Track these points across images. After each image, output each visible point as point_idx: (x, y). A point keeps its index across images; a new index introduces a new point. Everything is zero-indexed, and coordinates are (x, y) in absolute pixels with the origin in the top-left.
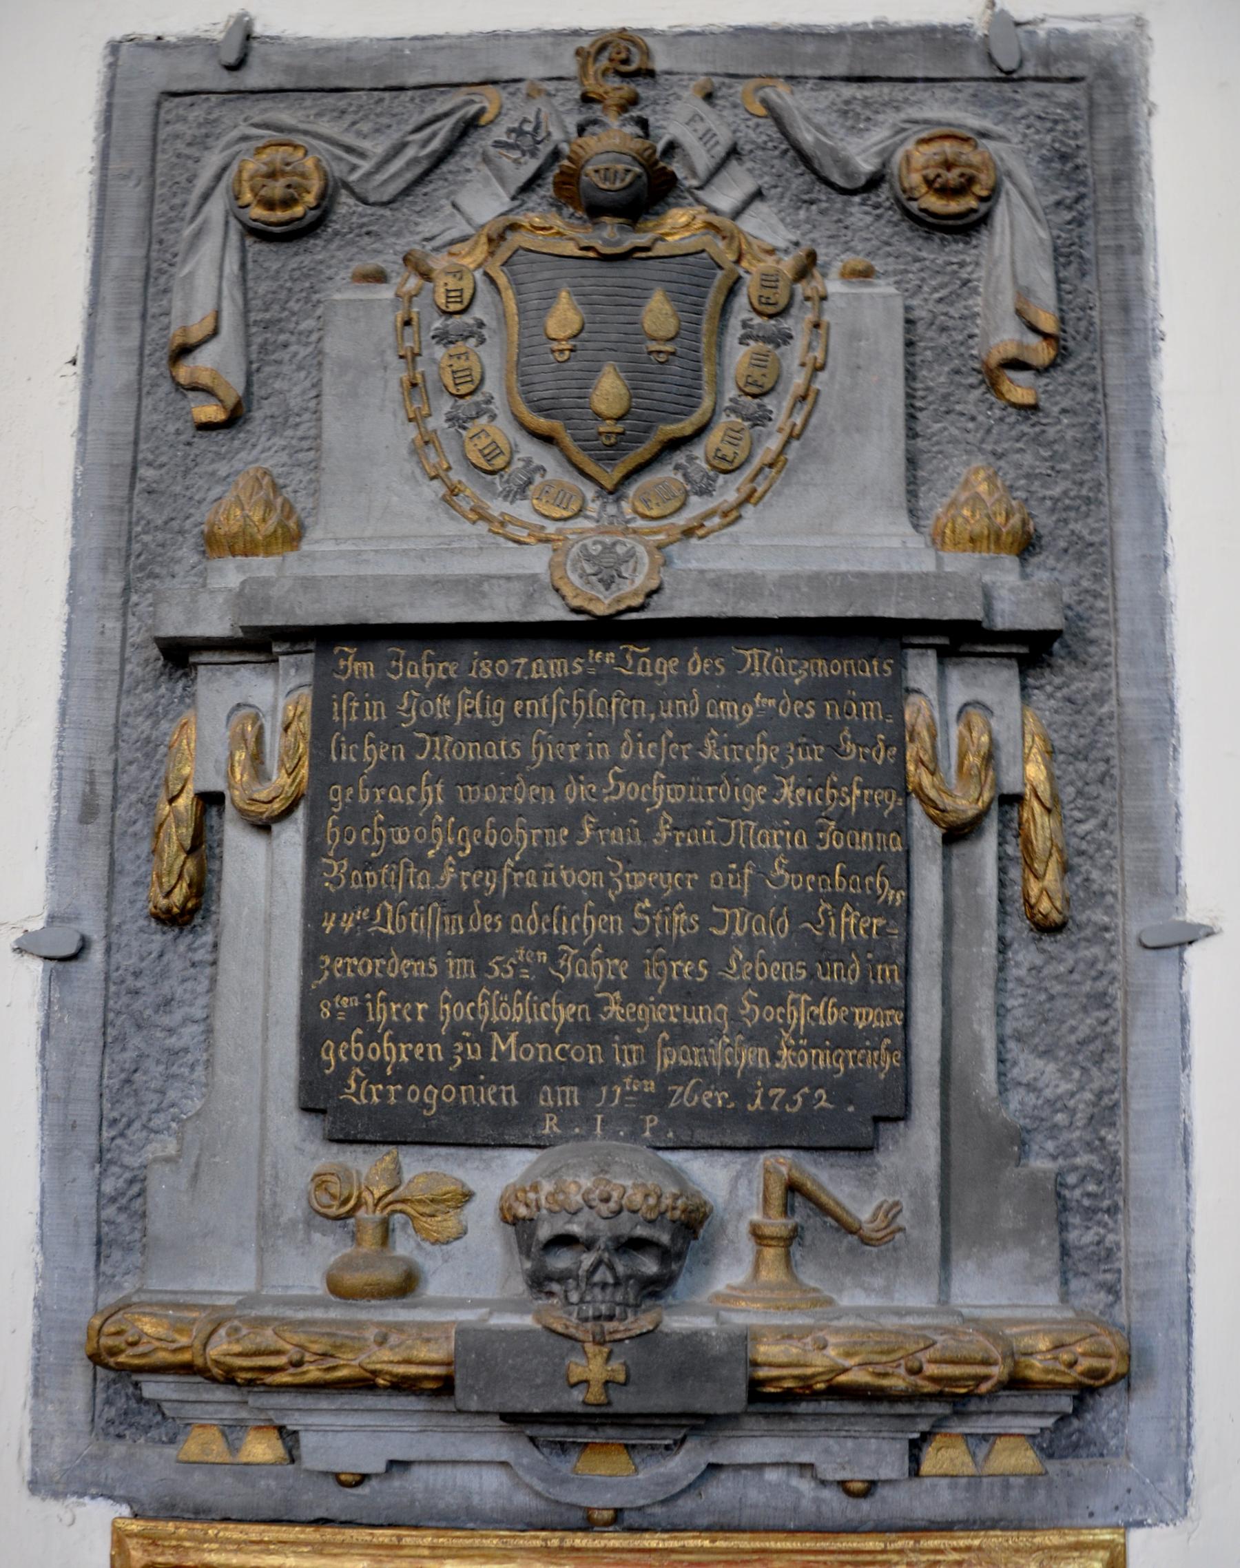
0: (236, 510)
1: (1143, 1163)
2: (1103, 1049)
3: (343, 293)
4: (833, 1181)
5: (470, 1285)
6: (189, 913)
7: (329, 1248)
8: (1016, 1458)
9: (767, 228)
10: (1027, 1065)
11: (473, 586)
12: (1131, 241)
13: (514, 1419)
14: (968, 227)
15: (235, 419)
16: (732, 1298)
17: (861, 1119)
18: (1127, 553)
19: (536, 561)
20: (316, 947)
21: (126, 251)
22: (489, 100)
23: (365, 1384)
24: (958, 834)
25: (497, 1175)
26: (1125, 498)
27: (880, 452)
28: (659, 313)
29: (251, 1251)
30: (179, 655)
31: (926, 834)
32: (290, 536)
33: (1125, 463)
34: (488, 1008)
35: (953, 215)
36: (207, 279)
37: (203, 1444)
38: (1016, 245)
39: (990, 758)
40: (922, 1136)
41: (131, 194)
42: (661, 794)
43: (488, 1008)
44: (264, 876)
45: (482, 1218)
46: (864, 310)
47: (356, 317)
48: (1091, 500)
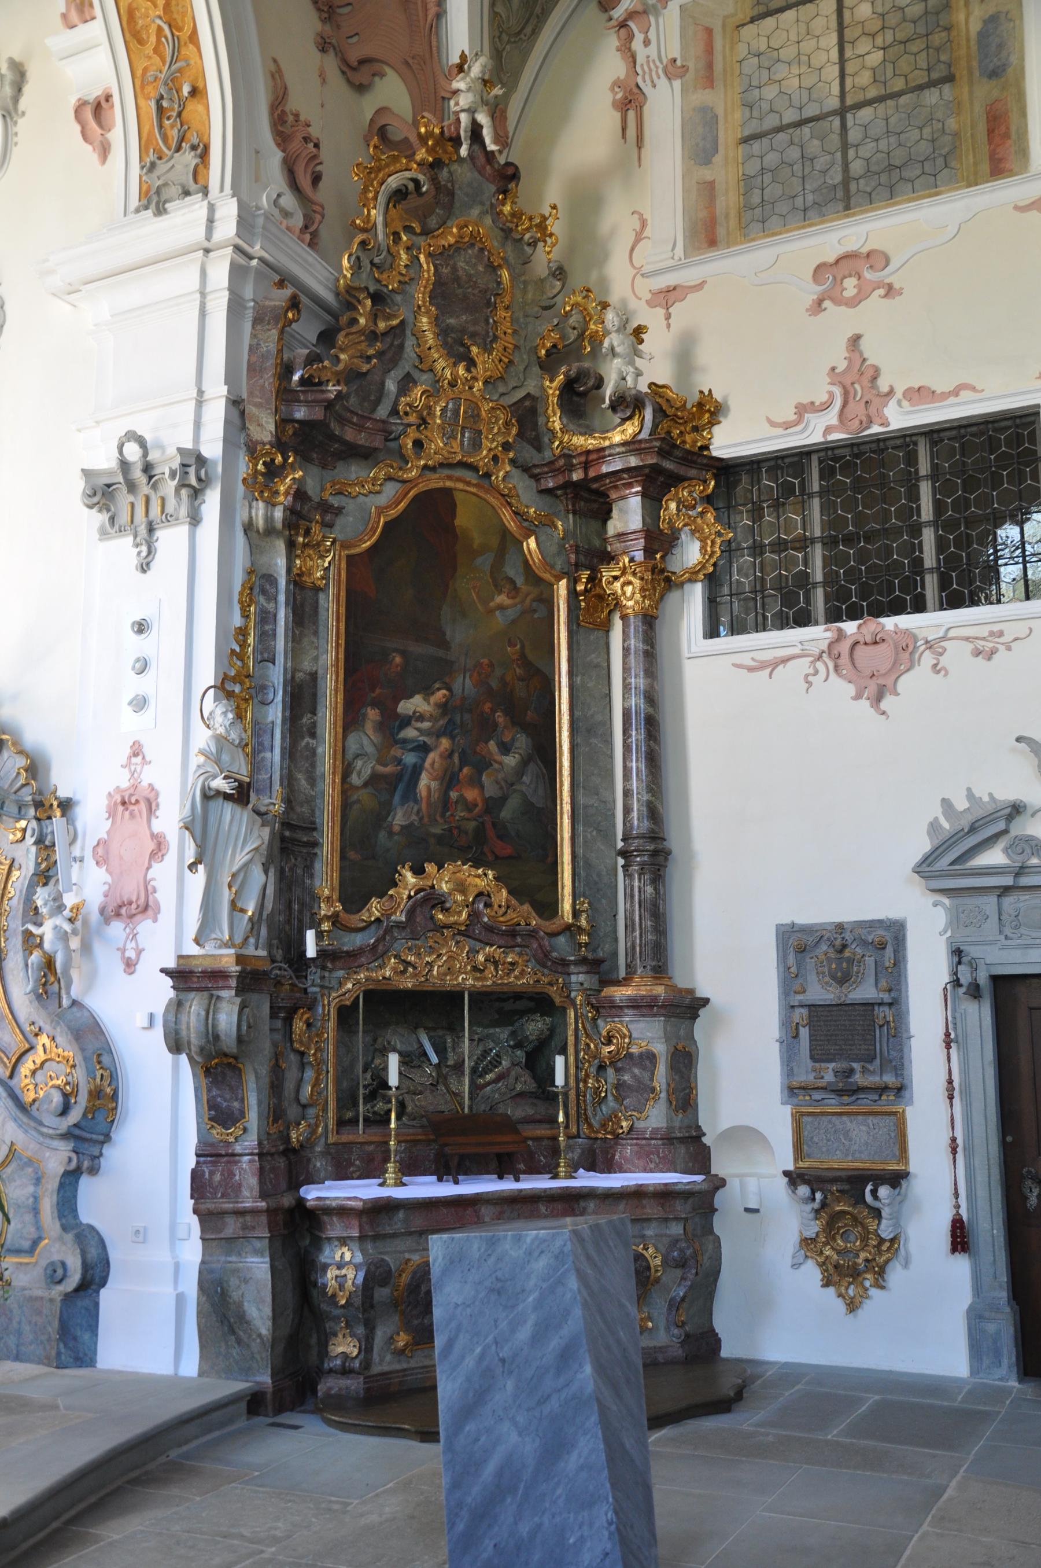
0: (797, 988)
1: (906, 1064)
2: (901, 1050)
3: (808, 960)
4: (868, 1066)
5: (829, 1077)
6: (796, 1036)
7: (814, 1074)
8: (892, 1098)
9: (858, 950)
10: (892, 1052)
11: (825, 1000)
12: (905, 949)
13: (833, 1091)
14: (884, 948)
15: (797, 976)
16: (858, 1078)
17: (871, 1059)
18: (903, 990)
19: (832, 996)
20: (811, 1041)
21: (781, 953)
22: (824, 932)
23: (818, 1088)
24: (881, 1026)
25: (832, 1065)
26: (903, 983)
27: (872, 980)
28: (845, 965)
29: (805, 1076)
30: (793, 1007)
31: (877, 1027)
32: (804, 992)
33: (903, 979)
34: (829, 1047)
35: (882, 946)
36: (791, 960)
37: (801, 1098)
38: (889, 951)
39: (885, 1017)
40: (878, 1061)
41: (781, 945)
42: (847, 1023)
43: (829, 1047)
44: (804, 1032)
45: (830, 1070)
46: (870, 961)
47: (810, 963)
48: (899, 984)
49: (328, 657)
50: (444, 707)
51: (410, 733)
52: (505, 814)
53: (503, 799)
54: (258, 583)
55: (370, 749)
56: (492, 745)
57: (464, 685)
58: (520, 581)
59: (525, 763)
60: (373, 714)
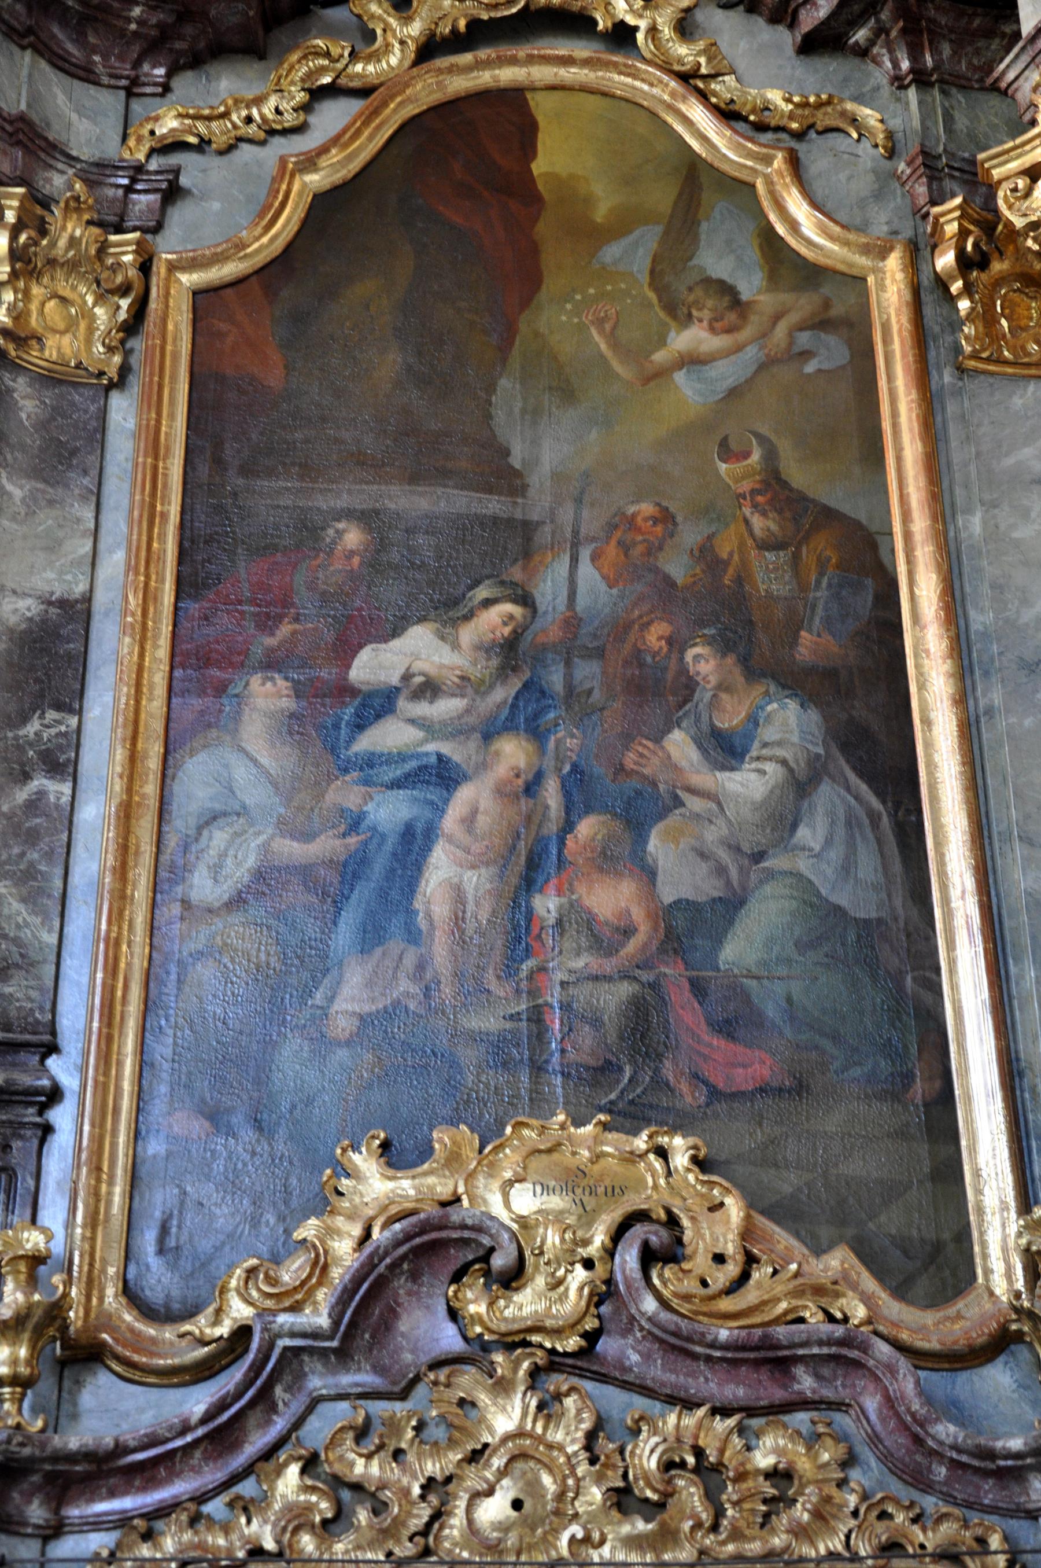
50: (510, 651)
51: (391, 735)
52: (739, 949)
53: (731, 906)
55: (252, 791)
56: (680, 745)
58: (750, 284)
59: (801, 785)
60: (267, 696)
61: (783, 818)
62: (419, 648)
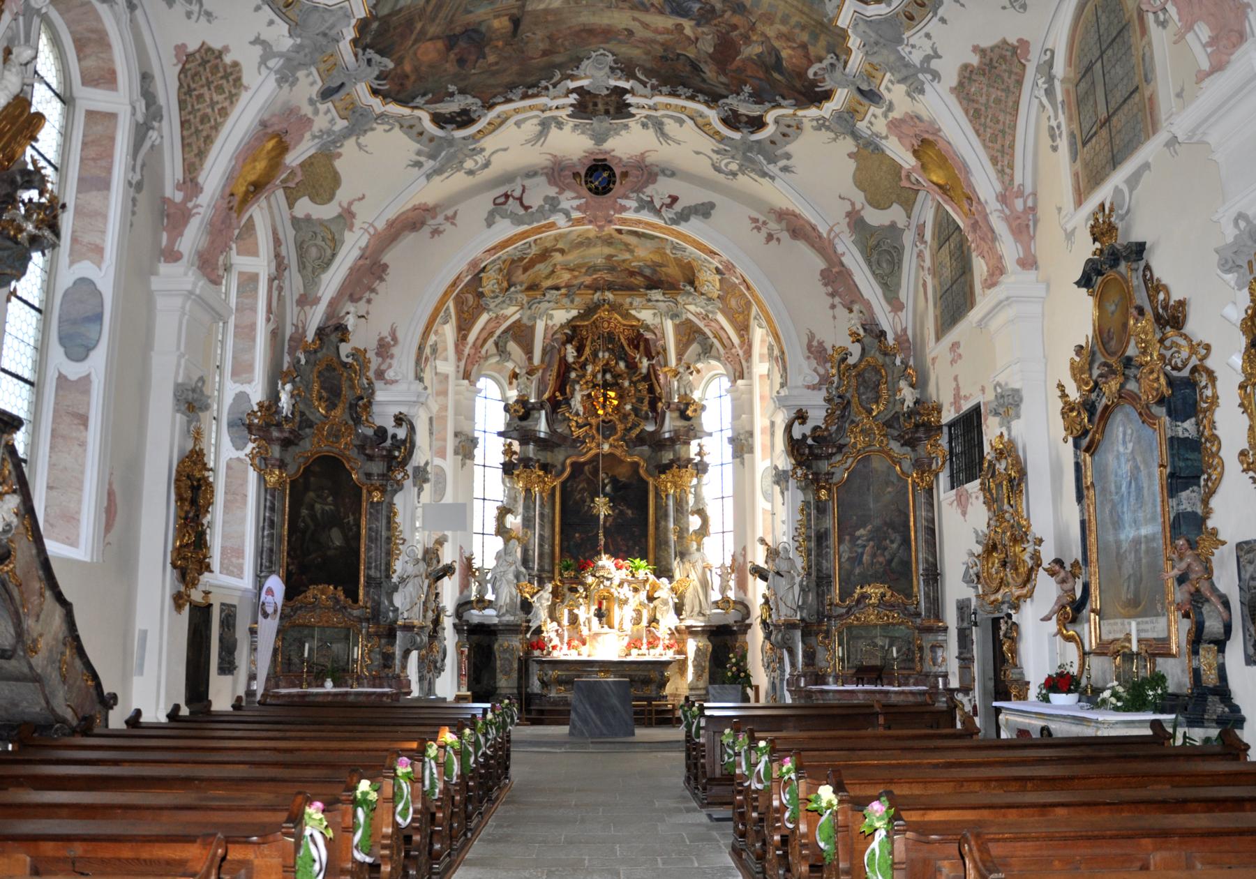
49: (830, 522)
51: (859, 542)
52: (893, 564)
54: (806, 504)
57: (878, 522)
59: (900, 546)
60: (847, 538)
61: (899, 548)
62: (861, 532)
